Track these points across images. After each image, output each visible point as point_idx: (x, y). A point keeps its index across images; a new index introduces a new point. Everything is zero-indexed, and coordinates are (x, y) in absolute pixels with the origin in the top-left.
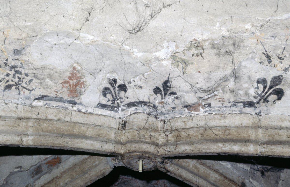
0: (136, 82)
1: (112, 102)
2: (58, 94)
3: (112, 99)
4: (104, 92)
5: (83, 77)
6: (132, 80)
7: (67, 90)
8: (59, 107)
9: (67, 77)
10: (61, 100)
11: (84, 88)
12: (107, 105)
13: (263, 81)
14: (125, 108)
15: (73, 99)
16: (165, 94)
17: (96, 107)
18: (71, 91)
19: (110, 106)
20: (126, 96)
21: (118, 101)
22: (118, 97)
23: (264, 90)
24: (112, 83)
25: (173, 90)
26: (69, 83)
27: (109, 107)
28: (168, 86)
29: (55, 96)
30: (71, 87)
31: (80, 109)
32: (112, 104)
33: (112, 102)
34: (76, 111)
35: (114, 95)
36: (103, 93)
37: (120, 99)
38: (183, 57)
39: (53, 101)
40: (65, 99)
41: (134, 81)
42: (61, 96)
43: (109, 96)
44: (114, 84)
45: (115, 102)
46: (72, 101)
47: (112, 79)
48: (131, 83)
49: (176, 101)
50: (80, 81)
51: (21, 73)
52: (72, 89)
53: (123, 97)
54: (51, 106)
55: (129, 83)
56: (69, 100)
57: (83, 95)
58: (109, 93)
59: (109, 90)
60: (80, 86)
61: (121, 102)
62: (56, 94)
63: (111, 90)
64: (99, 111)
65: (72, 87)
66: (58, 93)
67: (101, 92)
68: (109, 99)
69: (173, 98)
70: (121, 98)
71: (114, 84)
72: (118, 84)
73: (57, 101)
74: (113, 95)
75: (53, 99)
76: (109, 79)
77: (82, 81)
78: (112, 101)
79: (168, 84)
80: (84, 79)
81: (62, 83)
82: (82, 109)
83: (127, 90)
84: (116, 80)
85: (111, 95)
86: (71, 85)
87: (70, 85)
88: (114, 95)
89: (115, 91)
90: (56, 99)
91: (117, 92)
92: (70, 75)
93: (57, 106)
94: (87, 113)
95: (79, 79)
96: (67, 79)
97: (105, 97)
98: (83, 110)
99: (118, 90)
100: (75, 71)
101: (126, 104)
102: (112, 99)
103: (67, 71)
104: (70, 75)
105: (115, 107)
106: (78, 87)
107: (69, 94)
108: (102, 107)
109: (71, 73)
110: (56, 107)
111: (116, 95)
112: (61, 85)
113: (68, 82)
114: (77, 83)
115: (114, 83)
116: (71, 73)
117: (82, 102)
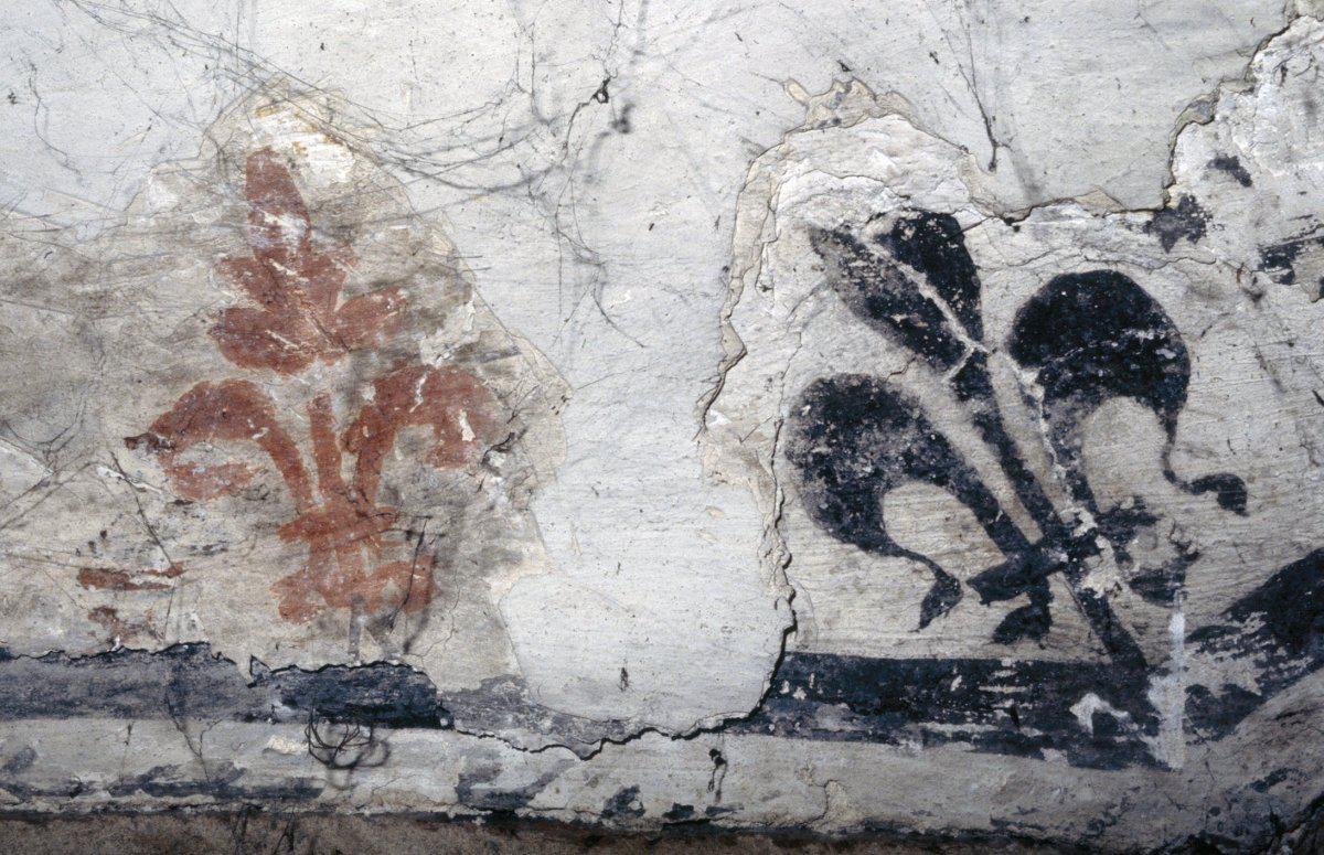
0: (1271, 176)
1: (999, 611)
2: (131, 607)
3: (978, 555)
4: (828, 474)
5: (431, 294)
6: (1191, 173)
7: (252, 518)
8: (171, 789)
9: (204, 339)
11: (498, 460)
12: (932, 672)
14: (1245, 674)
15: (371, 652)
17: (755, 720)
18: (310, 530)
19: (977, 670)
20: (1193, 469)
21: (1100, 578)
22: (1066, 508)
24: (900, 307)
26: (263, 419)
27: (974, 701)
29: (93, 638)
30: (294, 471)
31: (508, 783)
32: (1007, 633)
33: (999, 611)
34: (443, 818)
35: (1002, 489)
36: (819, 485)
37: (1119, 540)
39: (65, 708)
40: (243, 666)
41: (1228, 165)
42: (182, 620)
44: (941, 304)
45: (1043, 598)
46: (372, 684)
47: (881, 239)
48: (1197, 231)
50: (405, 361)
52: (319, 500)
53: (1161, 495)
54: (44, 786)
55: (1168, 240)
56: (309, 662)
57: (512, 560)
58: (915, 469)
59: (901, 422)
60: (427, 430)
61: (1157, 587)
62: (110, 612)
63: (922, 423)
65: (308, 463)
66: (128, 586)
67: (785, 470)
68: (947, 564)
70: (1126, 522)
71: (941, 304)
72: (1002, 302)
73: (126, 712)
74: (977, 498)
75: (63, 685)
76: (843, 238)
77: (432, 350)
78: (991, 587)
80: (463, 324)
81: (154, 444)
82: (541, 784)
83: (1183, 361)
84: (949, 226)
85: (945, 497)
86: (294, 436)
87: (280, 447)
88: (1002, 489)
89: (990, 427)
90: (117, 674)
91: (1032, 435)
92: (233, 295)
93: (146, 783)
94: (634, 825)
95: (391, 331)
96: (214, 367)
97: (866, 546)
98: (559, 800)
99: (1039, 393)
100: (290, 226)
101: (1240, 610)
102: (979, 554)
103: (177, 234)
104: (233, 295)
105: (1075, 679)
106: (397, 465)
107: (289, 582)
108: (857, 708)
109: (237, 266)
110: (129, 791)
111: (1030, 478)
112: (149, 469)
114: (369, 394)
115: (928, 292)
116: (237, 266)
117: (513, 669)
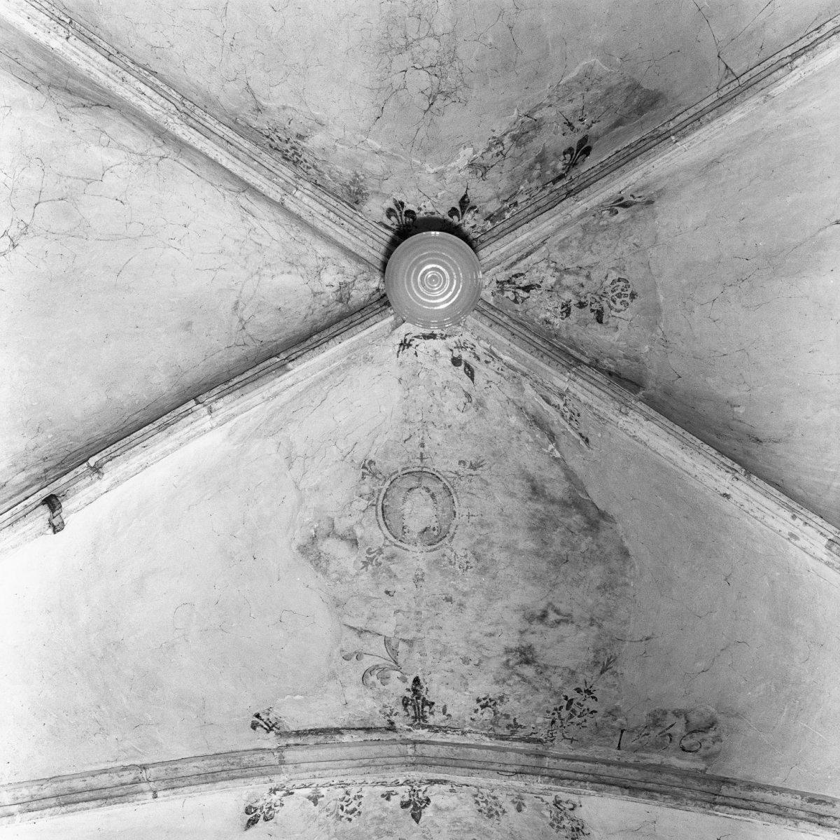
6: (422, 206)
13: (570, 150)
16: (463, 213)
23: (572, 157)
25: (471, 204)
28: (465, 202)
38: (482, 162)
41: (425, 206)
43: (393, 218)
49: (477, 216)
51: (300, 156)
69: (472, 213)
74: (398, 220)
79: (466, 199)
96: (348, 184)
113: (348, 187)
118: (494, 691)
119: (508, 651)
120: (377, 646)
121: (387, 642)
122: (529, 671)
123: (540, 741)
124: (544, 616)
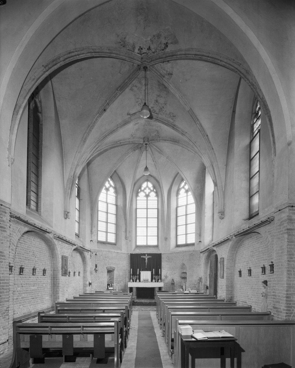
10: (131, 51)
64: (138, 55)
118: (153, 106)
119: (155, 100)
120: (140, 100)
121: (141, 99)
122: (157, 103)
123: (157, 114)
124: (159, 96)
